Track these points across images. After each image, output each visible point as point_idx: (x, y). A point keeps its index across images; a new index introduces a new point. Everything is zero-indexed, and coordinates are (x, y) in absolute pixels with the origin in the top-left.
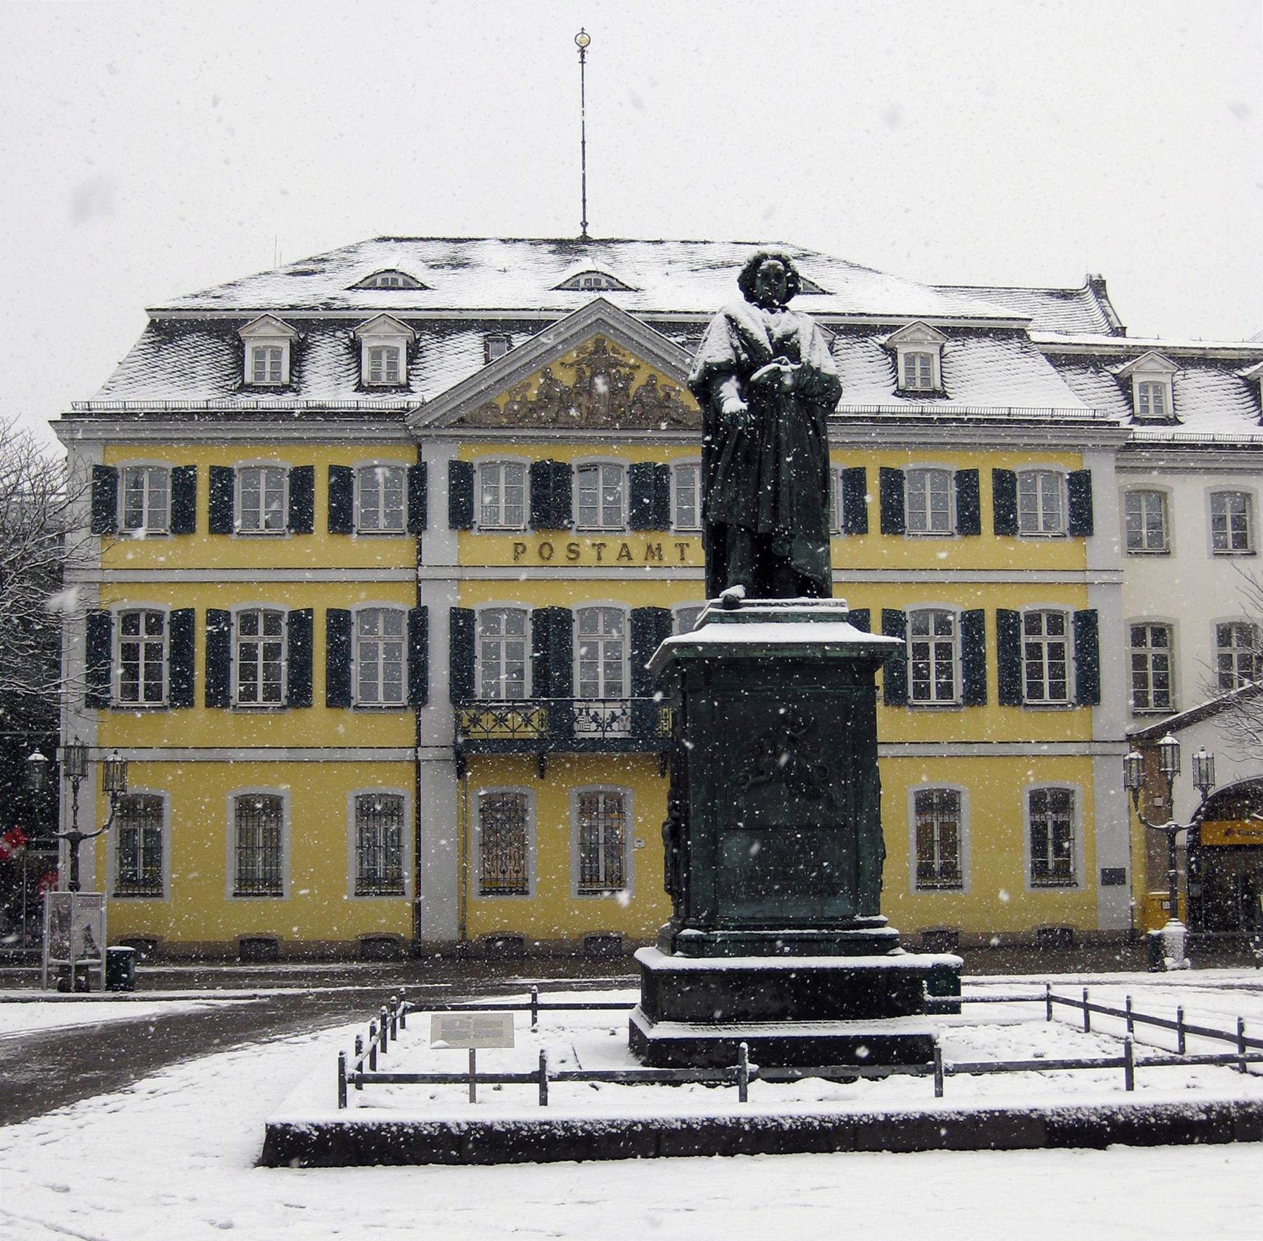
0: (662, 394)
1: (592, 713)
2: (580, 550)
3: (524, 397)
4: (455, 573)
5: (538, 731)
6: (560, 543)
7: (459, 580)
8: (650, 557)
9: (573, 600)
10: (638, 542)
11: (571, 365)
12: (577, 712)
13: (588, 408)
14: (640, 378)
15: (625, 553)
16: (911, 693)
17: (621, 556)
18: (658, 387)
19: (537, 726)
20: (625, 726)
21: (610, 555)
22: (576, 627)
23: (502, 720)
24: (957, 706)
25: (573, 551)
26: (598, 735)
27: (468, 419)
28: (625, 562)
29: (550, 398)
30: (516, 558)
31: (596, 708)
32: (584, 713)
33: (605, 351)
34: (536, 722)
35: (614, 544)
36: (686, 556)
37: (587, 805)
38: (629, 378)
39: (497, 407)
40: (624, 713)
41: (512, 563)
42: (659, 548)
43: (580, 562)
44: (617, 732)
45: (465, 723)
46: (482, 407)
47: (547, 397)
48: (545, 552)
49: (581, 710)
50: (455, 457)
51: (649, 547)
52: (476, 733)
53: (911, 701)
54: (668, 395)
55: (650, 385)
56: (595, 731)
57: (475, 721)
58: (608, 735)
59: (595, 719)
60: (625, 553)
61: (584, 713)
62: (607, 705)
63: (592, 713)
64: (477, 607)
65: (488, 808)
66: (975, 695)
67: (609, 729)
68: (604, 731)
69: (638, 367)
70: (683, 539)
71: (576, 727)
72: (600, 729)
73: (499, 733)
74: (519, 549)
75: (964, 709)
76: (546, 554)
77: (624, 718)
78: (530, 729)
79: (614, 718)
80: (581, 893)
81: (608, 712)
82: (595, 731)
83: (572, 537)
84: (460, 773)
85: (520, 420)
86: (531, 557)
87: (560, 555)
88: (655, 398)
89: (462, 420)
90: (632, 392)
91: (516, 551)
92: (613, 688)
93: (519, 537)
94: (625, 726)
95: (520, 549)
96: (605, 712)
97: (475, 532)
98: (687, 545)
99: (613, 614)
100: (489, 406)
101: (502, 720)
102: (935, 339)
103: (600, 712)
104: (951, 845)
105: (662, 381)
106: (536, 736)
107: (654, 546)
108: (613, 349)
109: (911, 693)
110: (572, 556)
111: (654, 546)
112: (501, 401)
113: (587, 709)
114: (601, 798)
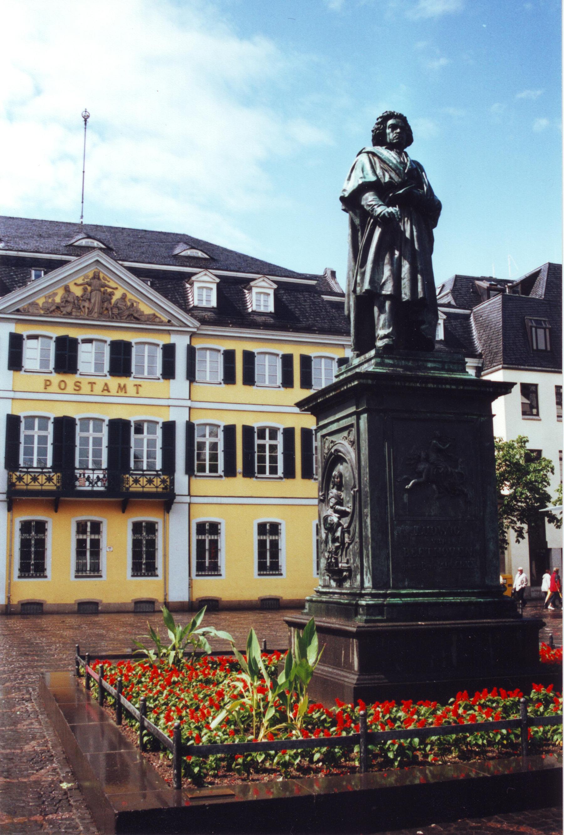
0: (129, 304)
1: (86, 476)
2: (82, 385)
3: (54, 300)
4: (11, 395)
5: (56, 485)
6: (70, 379)
7: (13, 399)
8: (120, 391)
9: (76, 412)
10: (114, 382)
11: (81, 285)
12: (78, 475)
13: (88, 308)
14: (118, 295)
15: (106, 388)
16: (256, 471)
17: (104, 390)
18: (127, 300)
19: (55, 483)
20: (104, 484)
21: (98, 388)
22: (78, 428)
23: (35, 479)
24: (280, 478)
25: (78, 386)
26: (90, 488)
27: (21, 310)
28: (106, 393)
29: (67, 301)
30: (46, 388)
31: (88, 473)
32: (82, 476)
33: (99, 279)
34: (55, 481)
35: (100, 382)
36: (140, 392)
37: (81, 528)
38: (111, 294)
39: (37, 304)
40: (104, 477)
41: (44, 391)
42: (125, 386)
43: (81, 392)
44: (100, 487)
45: (14, 480)
46: (30, 304)
47: (66, 301)
48: (62, 387)
49: (80, 475)
50: (13, 331)
51: (119, 386)
52: (20, 486)
53: (256, 475)
54: (132, 304)
55: (124, 297)
56: (88, 486)
57: (20, 479)
58: (95, 489)
59: (88, 479)
60: (106, 388)
61: (82, 476)
62: (95, 472)
63: (86, 476)
64: (22, 414)
65: (26, 527)
66: (289, 473)
67: (96, 485)
68: (93, 486)
69: (117, 288)
70: (138, 382)
71: (77, 483)
72: (91, 485)
73: (35, 486)
74: (48, 383)
75: (284, 480)
76: (63, 386)
77: (104, 479)
78: (51, 484)
79: (98, 479)
80: (76, 577)
81: (95, 476)
82: (88, 486)
83: (77, 377)
84: (10, 509)
85: (51, 312)
86: (54, 387)
87: (70, 387)
88: (125, 306)
89: (18, 310)
90: (113, 301)
91: (46, 383)
92: (98, 463)
93: (48, 376)
94: (104, 484)
95: (48, 383)
96: (93, 477)
97: (22, 373)
98: (140, 385)
99: (98, 421)
100: (34, 304)
101: (35, 479)
103: (91, 476)
104: (275, 553)
105: (129, 296)
106: (55, 488)
107: (122, 386)
108: (104, 278)
109: (256, 471)
110: (77, 388)
111: (122, 386)
112: (41, 302)
113: (84, 474)
114: (89, 524)
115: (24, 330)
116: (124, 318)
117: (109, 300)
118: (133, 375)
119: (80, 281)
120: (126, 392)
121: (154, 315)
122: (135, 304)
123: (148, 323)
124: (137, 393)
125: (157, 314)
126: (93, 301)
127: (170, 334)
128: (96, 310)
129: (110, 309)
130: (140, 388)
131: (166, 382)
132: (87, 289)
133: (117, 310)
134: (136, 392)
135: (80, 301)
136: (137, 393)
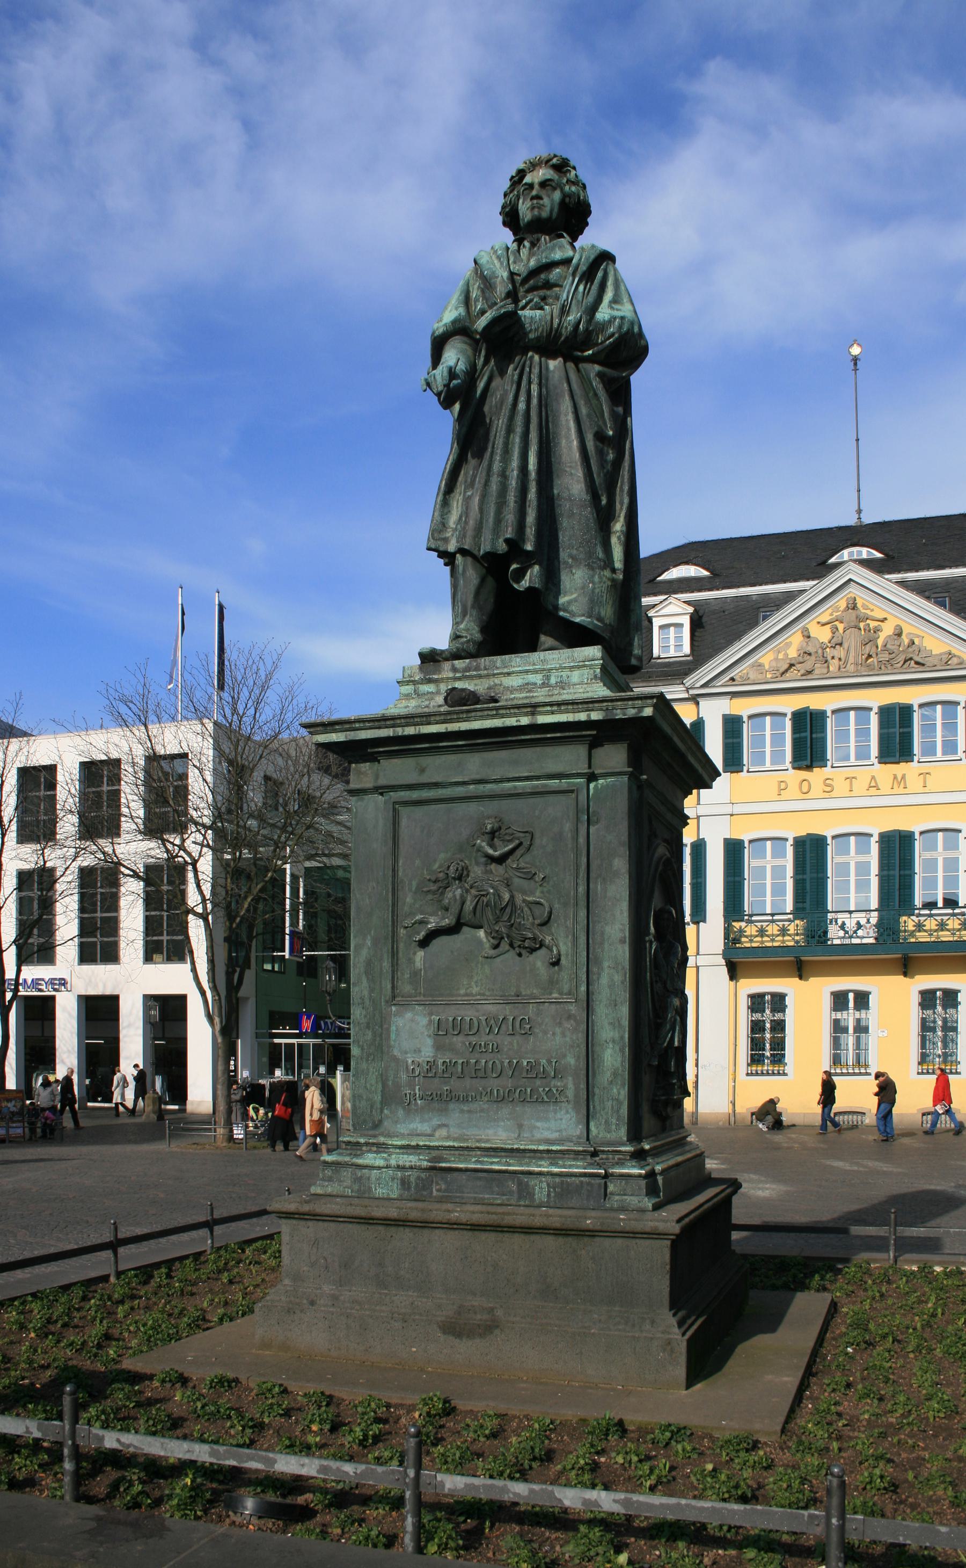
115: (744, 708)
117: (872, 641)
119: (825, 618)
126: (846, 645)
128: (851, 660)
129: (874, 655)
132: (837, 629)
133: (887, 655)
135: (828, 650)
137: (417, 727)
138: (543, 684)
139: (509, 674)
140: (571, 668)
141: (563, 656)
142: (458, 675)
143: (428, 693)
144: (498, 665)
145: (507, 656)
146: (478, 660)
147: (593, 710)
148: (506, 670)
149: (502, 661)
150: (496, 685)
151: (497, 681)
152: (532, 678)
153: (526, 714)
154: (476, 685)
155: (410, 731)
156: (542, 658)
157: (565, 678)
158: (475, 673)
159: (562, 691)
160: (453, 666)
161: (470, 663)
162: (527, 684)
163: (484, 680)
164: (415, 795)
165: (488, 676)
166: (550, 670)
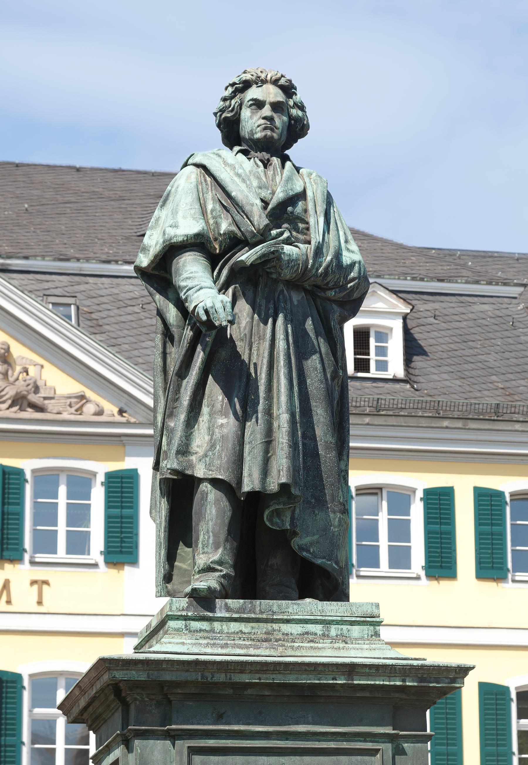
54: (26, 371)
70: (41, 573)
98: (46, 582)
102: (396, 306)
116: (6, 405)
118: (27, 557)
120: (9, 602)
121: (82, 397)
122: (32, 371)
123: (66, 416)
124: (40, 603)
125: (90, 394)
127: (124, 445)
130: (45, 587)
131: (113, 572)
134: (36, 599)
136: (40, 603)
137: (228, 675)
138: (324, 635)
139: (288, 621)
140: (352, 623)
141: (341, 609)
142: (235, 616)
143: (201, 630)
144: (275, 609)
145: (284, 602)
146: (254, 601)
147: (408, 676)
148: (285, 617)
149: (279, 606)
150: (274, 631)
151: (276, 626)
152: (311, 628)
153: (343, 674)
154: (252, 628)
155: (221, 677)
156: (320, 608)
157: (345, 632)
158: (253, 616)
159: (347, 645)
160: (226, 604)
161: (245, 603)
162: (307, 633)
163: (261, 625)
164: (211, 743)
165: (266, 621)
166: (331, 622)
